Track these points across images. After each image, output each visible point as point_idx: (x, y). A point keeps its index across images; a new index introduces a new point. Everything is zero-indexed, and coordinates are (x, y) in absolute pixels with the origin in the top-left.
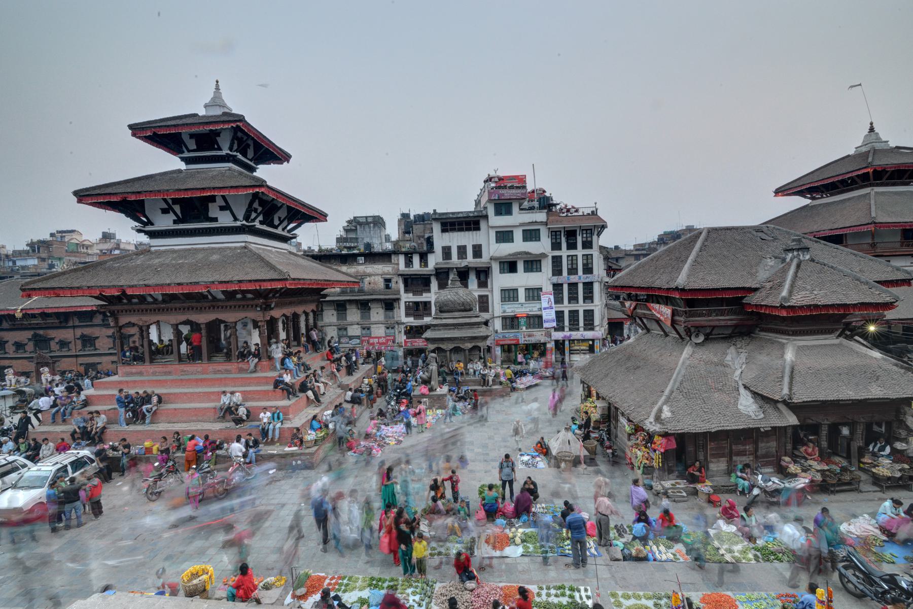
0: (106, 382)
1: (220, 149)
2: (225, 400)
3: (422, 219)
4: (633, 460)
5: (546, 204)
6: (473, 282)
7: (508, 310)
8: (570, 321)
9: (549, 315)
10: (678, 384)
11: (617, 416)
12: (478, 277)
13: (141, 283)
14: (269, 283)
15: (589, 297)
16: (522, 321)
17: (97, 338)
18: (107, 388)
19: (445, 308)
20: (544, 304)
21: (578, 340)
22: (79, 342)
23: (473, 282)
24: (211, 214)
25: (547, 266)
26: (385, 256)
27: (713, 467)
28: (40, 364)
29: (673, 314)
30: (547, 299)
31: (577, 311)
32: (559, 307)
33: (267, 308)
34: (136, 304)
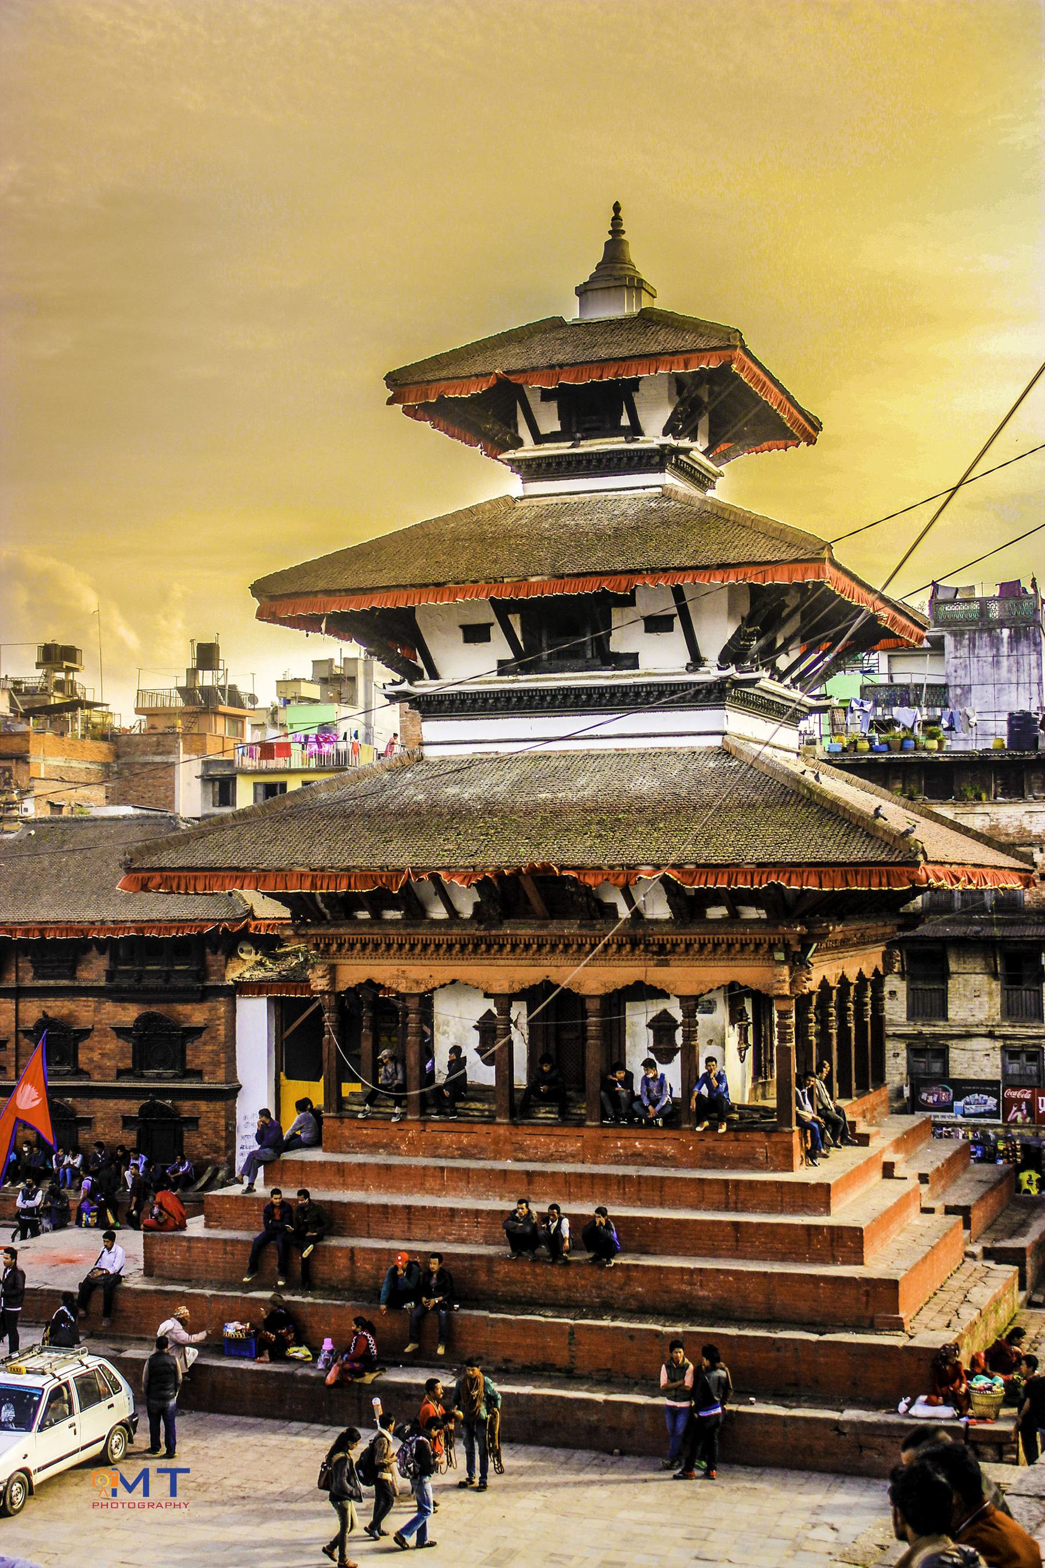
17: (86, 1033)
24: (619, 644)
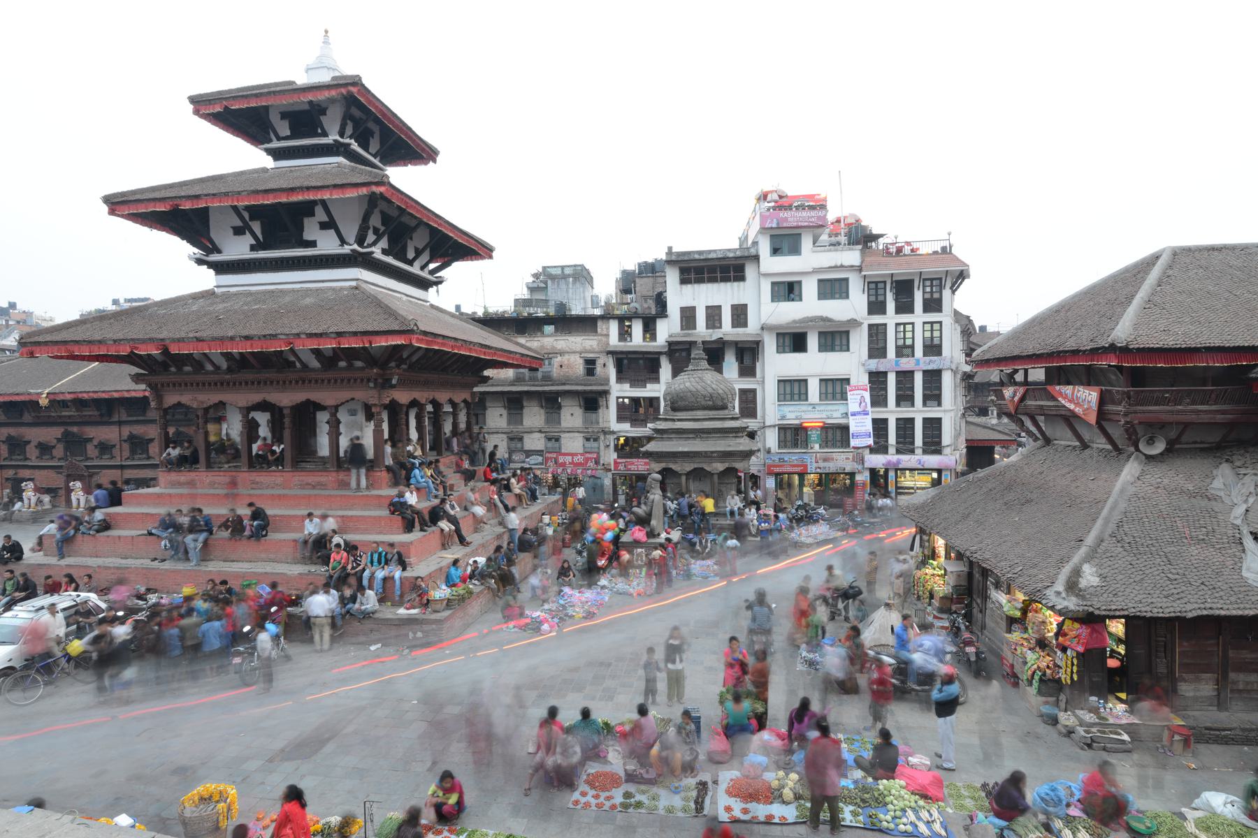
0: (140, 495)
1: (325, 134)
2: (312, 528)
3: (650, 269)
4: (1017, 669)
5: (862, 238)
6: (731, 365)
7: (789, 416)
8: (898, 436)
9: (861, 427)
10: (1112, 527)
11: (985, 588)
12: (740, 359)
13: (191, 335)
14: (384, 338)
15: (933, 395)
16: (814, 435)
18: (139, 504)
19: (681, 404)
20: (853, 406)
21: (911, 470)
22: (126, 446)
23: (731, 365)
24: (307, 236)
25: (860, 341)
26: (587, 323)
27: (1186, 689)
28: (71, 477)
29: (1102, 401)
30: (858, 398)
31: (912, 420)
32: (880, 413)
33: (385, 384)
34: (188, 373)
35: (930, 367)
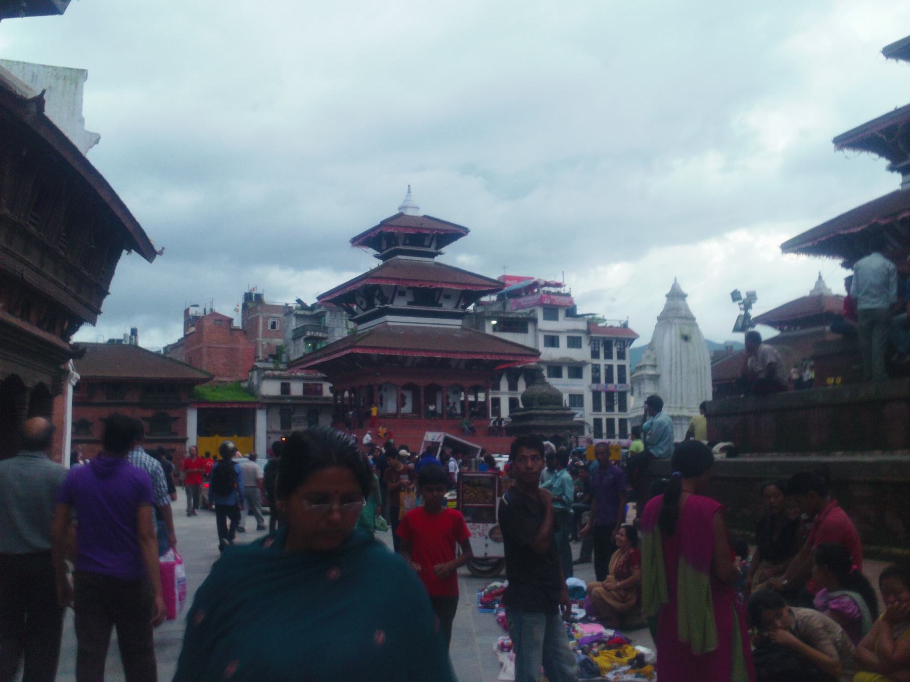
25: (587, 373)
35: (622, 390)
